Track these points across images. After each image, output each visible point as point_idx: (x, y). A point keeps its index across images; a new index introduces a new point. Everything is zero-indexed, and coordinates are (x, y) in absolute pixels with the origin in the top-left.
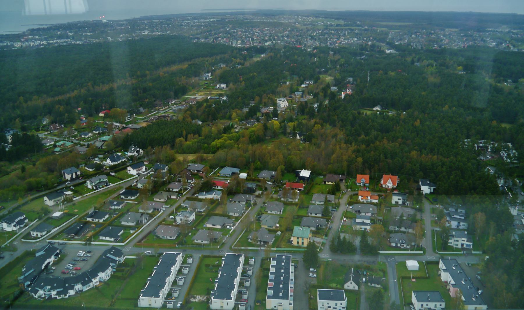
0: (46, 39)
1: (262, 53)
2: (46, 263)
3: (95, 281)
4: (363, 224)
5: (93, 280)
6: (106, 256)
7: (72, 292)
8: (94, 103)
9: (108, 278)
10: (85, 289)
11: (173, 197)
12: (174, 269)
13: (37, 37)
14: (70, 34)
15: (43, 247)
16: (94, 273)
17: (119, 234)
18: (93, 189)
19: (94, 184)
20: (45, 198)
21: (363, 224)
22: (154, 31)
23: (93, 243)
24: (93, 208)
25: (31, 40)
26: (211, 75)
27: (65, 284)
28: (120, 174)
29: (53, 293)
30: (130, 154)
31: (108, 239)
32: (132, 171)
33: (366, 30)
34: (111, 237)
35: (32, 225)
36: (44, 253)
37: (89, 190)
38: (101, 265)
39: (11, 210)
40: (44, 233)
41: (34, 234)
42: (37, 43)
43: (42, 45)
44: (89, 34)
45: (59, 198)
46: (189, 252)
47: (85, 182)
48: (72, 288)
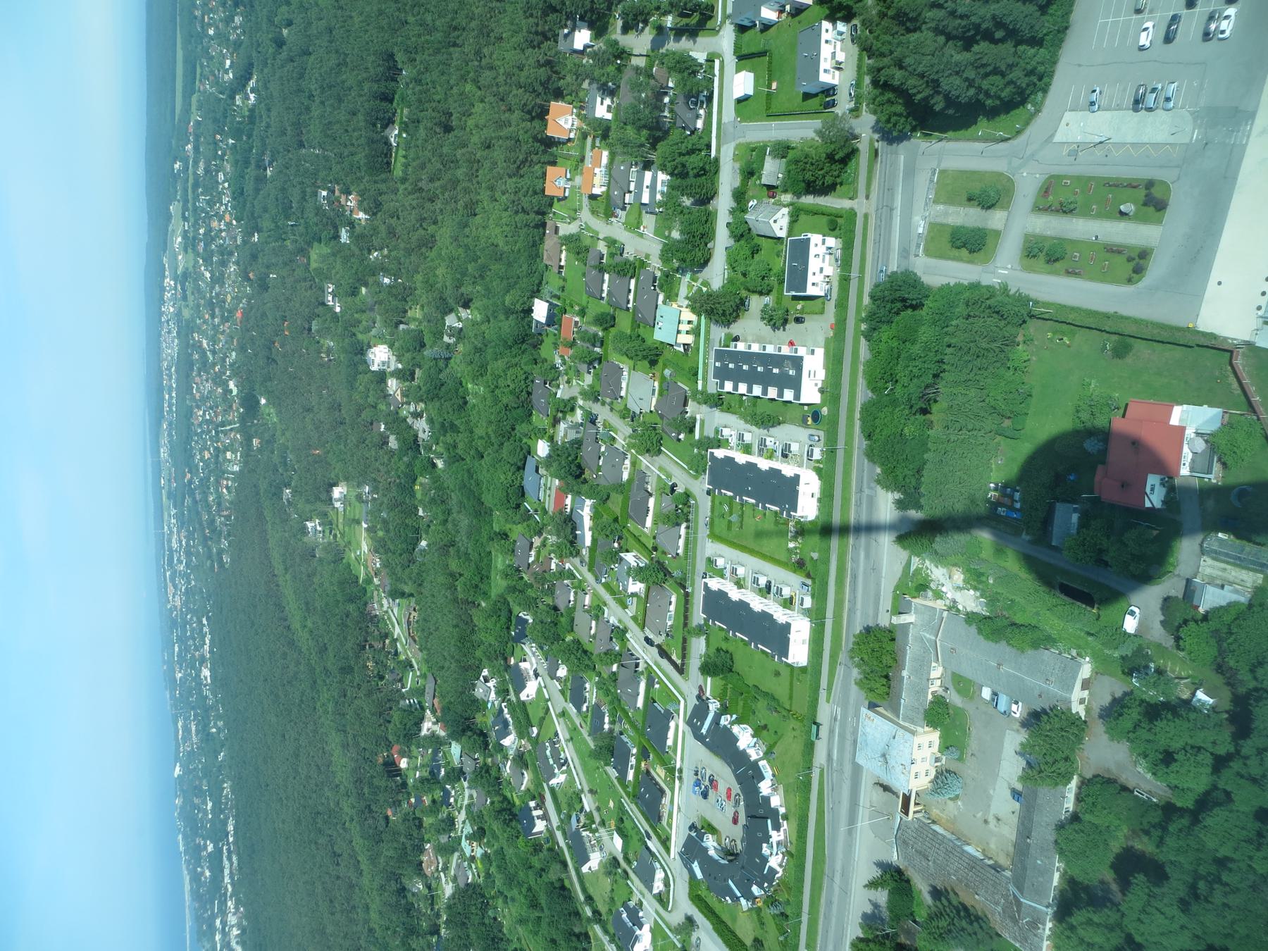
0: (223, 903)
1: (258, 402)
4: (653, 187)
7: (776, 801)
8: (376, 782)
11: (587, 600)
12: (735, 594)
13: (218, 922)
14: (210, 848)
16: (737, 759)
18: (569, 772)
20: (585, 869)
21: (653, 187)
22: (203, 656)
23: (678, 766)
25: (225, 934)
26: (310, 519)
27: (759, 816)
28: (535, 715)
29: (776, 837)
30: (493, 696)
31: (671, 734)
32: (530, 691)
33: (196, 149)
34: (668, 728)
37: (571, 780)
38: (722, 744)
40: (657, 865)
41: (658, 886)
42: (232, 920)
43: (237, 908)
44: (210, 805)
45: (586, 840)
46: (701, 566)
47: (552, 790)
48: (767, 800)
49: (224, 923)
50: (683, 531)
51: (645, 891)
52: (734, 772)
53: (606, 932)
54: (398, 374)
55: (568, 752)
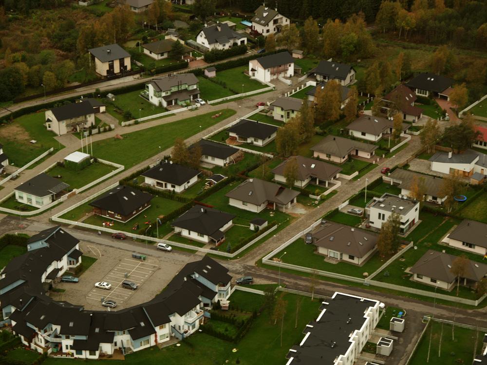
2: (50, 270)
3: (162, 334)
5: (157, 329)
6: (189, 277)
7: (107, 348)
9: (192, 331)
10: (139, 347)
15: (45, 232)
17: (222, 230)
19: (164, 94)
29: (67, 343)
31: (194, 236)
34: (201, 234)
36: (46, 245)
48: (110, 339)
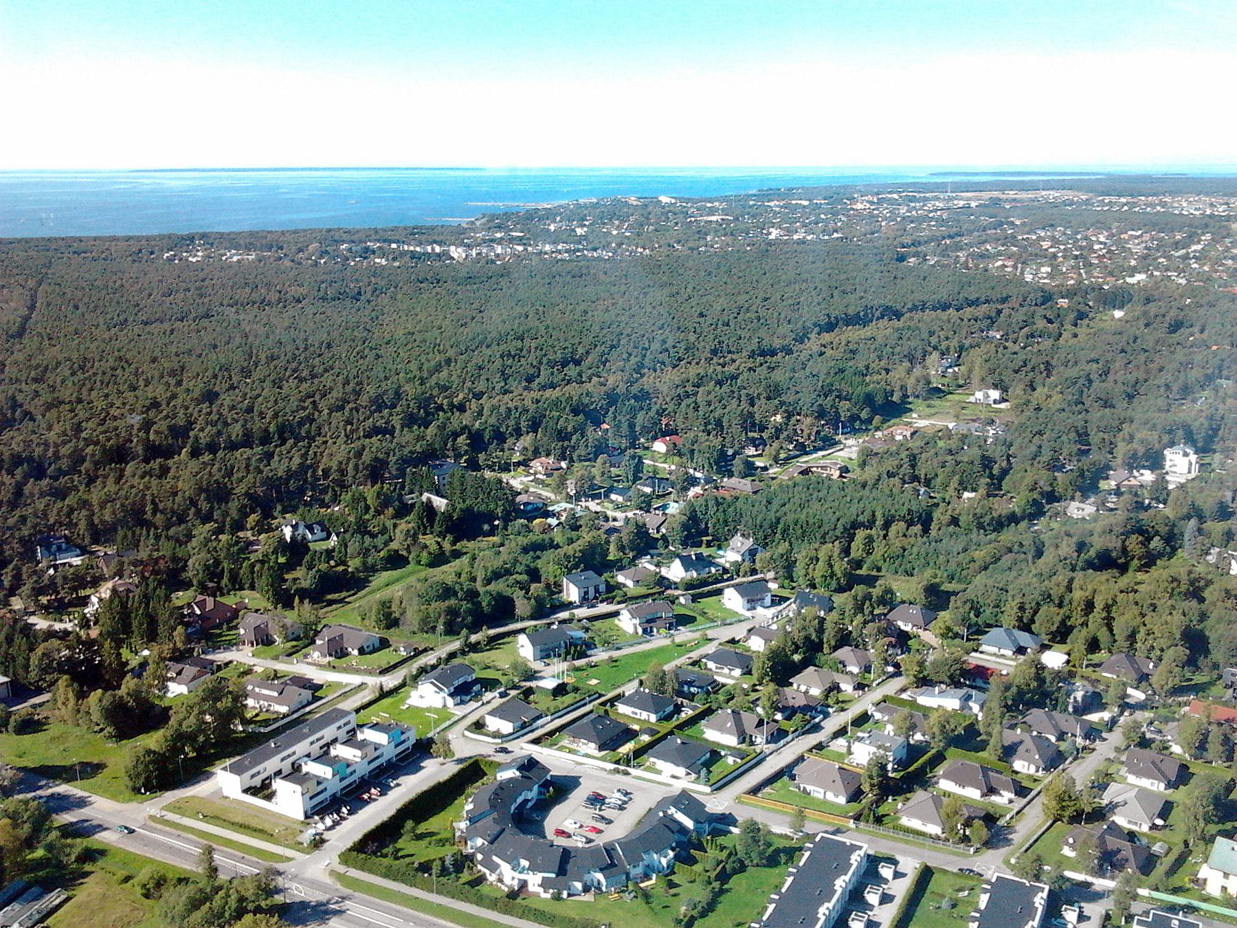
24: (636, 683)
35: (488, 702)
39: (444, 656)
41: (493, 723)
49: (500, 241)
50: (935, 829)
51: (489, 707)
52: (618, 841)
53: (452, 655)
54: (1161, 484)
55: (660, 640)
